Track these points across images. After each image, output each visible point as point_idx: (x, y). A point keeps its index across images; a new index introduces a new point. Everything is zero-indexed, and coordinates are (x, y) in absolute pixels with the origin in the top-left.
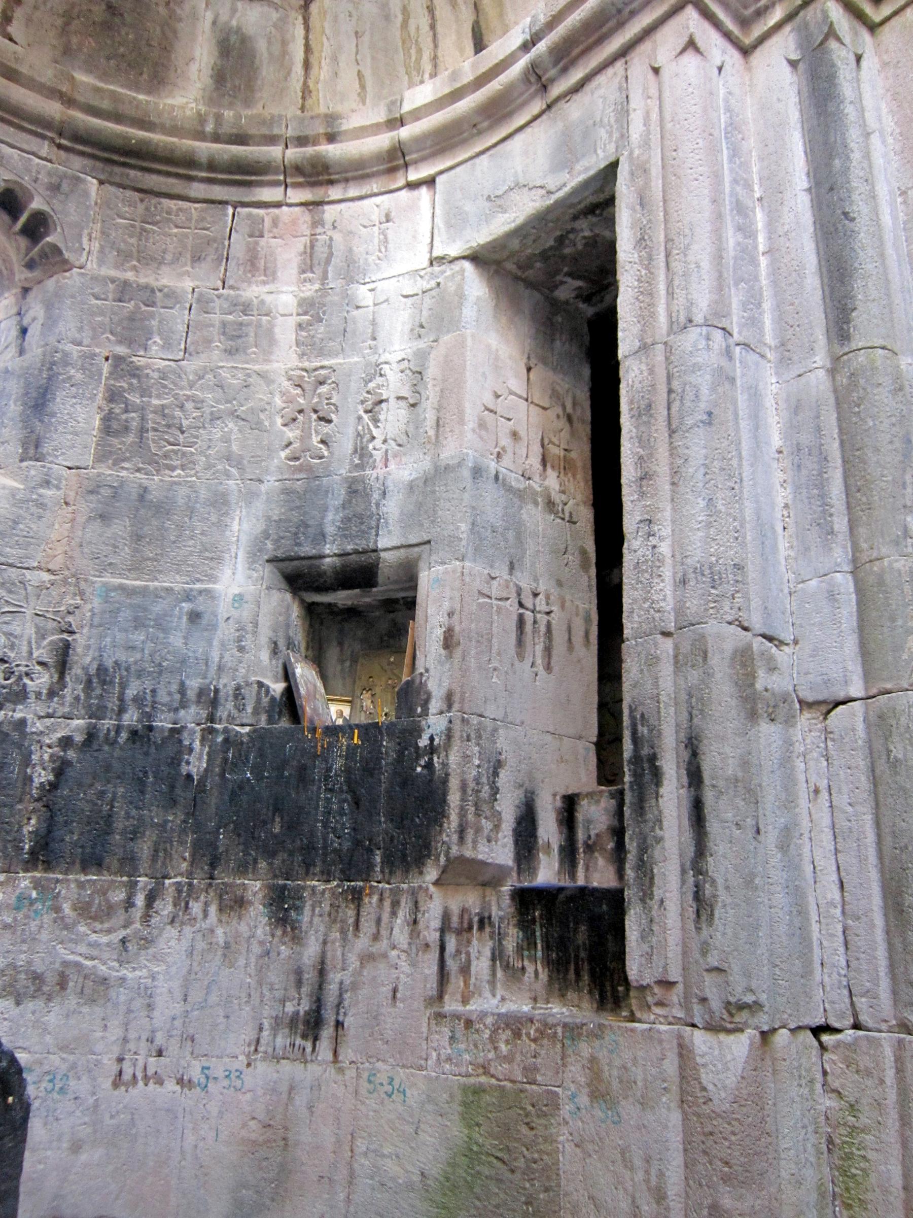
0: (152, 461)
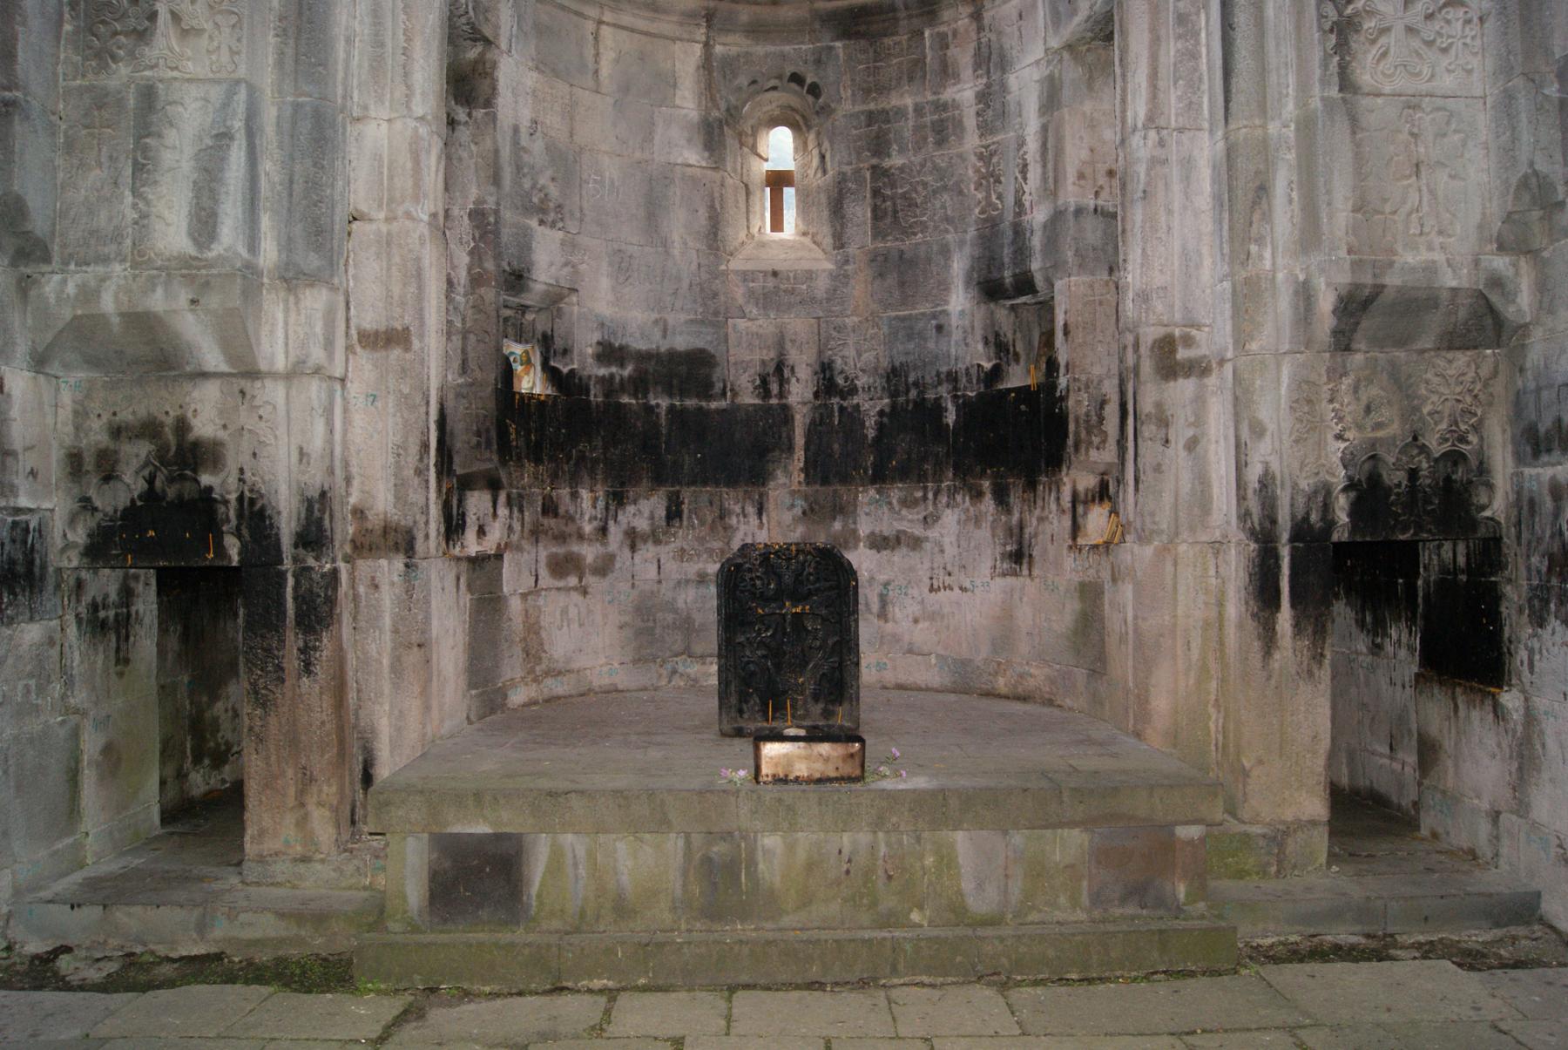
0: (904, 232)
